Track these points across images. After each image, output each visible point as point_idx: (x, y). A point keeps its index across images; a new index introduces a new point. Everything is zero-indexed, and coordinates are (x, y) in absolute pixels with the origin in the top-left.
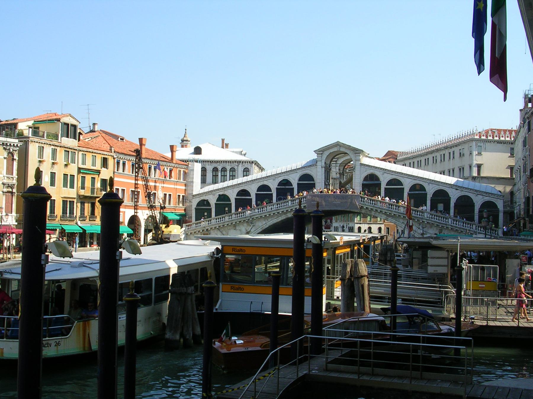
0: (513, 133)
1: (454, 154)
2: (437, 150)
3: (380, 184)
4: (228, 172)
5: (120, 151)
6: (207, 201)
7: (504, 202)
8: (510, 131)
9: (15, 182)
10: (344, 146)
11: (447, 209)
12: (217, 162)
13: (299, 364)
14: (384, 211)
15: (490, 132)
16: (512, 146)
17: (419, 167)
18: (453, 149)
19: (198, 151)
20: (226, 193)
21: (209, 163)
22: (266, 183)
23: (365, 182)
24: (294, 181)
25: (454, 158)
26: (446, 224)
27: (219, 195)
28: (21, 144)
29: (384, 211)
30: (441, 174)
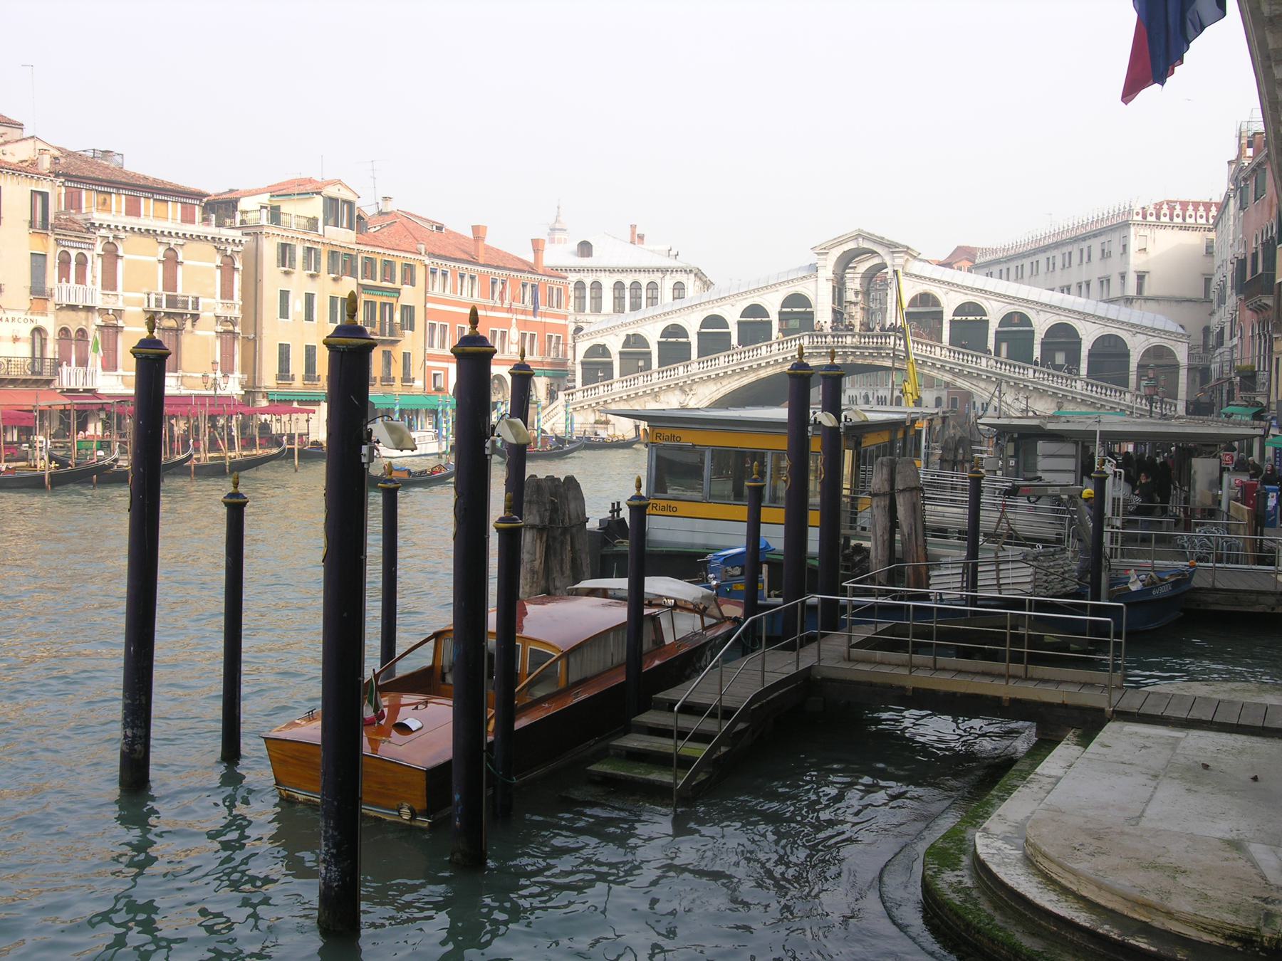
0: (1213, 209)
2: (1057, 245)
5: (437, 252)
6: (604, 346)
7: (1190, 348)
8: (1207, 206)
11: (1074, 359)
12: (623, 271)
15: (1165, 206)
17: (1019, 278)
19: (585, 248)
22: (717, 311)
23: (911, 310)
27: (628, 336)
28: (248, 238)
30: (1063, 291)
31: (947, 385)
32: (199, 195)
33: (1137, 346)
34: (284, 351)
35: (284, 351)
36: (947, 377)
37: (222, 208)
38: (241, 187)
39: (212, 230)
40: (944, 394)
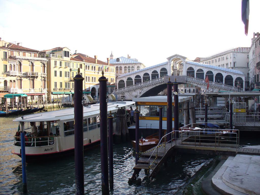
1: (224, 58)
3: (194, 71)
4: (131, 68)
7: (245, 78)
8: (247, 48)
9: (46, 76)
10: (179, 56)
11: (222, 81)
13: (172, 142)
14: (196, 82)
16: (248, 54)
18: (223, 56)
20: (131, 77)
21: (123, 65)
23: (188, 71)
24: (159, 70)
25: (224, 60)
26: (222, 87)
27: (128, 78)
28: (48, 60)
29: (196, 82)
31: (196, 86)
32: (37, 52)
33: (234, 77)
34: (56, 83)
35: (56, 83)
36: (196, 85)
37: (42, 54)
38: (45, 49)
39: (40, 59)
40: (195, 89)
